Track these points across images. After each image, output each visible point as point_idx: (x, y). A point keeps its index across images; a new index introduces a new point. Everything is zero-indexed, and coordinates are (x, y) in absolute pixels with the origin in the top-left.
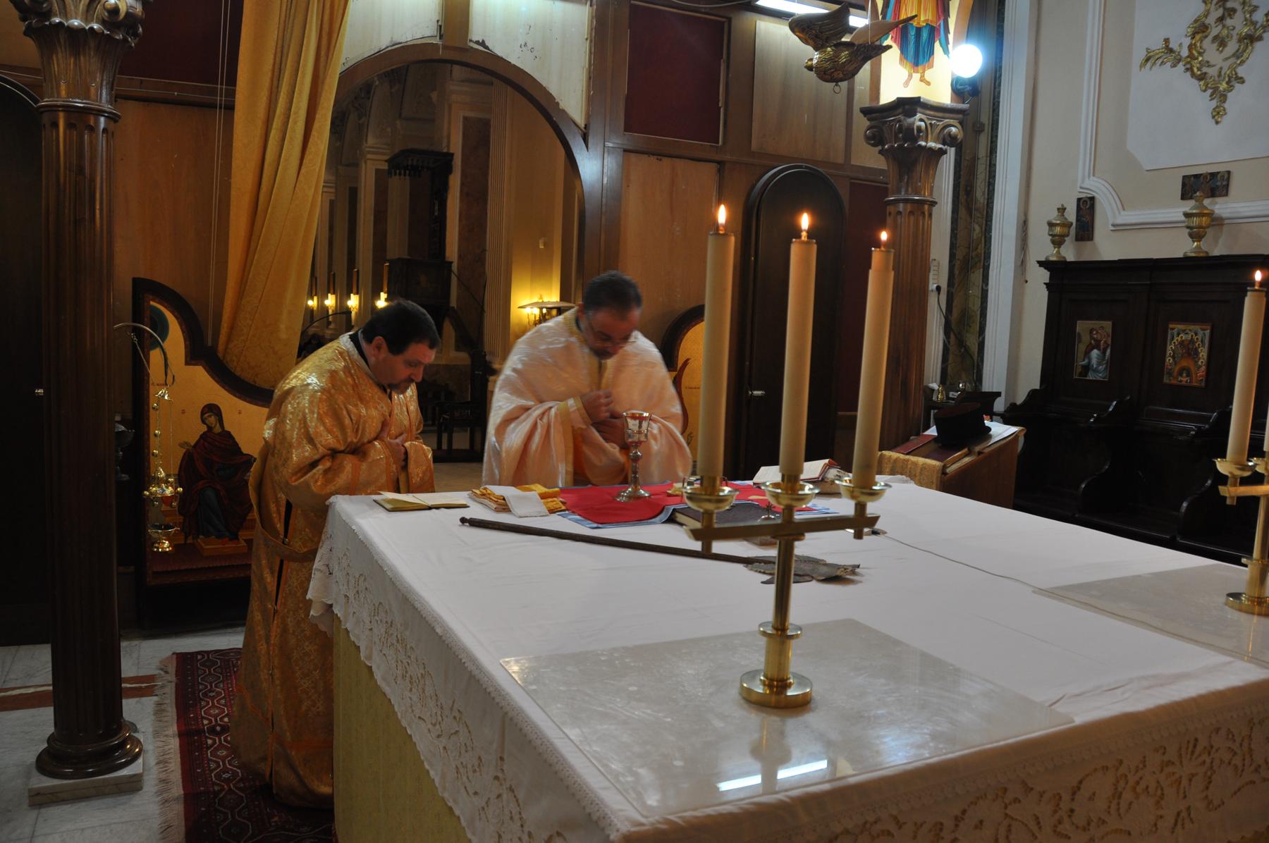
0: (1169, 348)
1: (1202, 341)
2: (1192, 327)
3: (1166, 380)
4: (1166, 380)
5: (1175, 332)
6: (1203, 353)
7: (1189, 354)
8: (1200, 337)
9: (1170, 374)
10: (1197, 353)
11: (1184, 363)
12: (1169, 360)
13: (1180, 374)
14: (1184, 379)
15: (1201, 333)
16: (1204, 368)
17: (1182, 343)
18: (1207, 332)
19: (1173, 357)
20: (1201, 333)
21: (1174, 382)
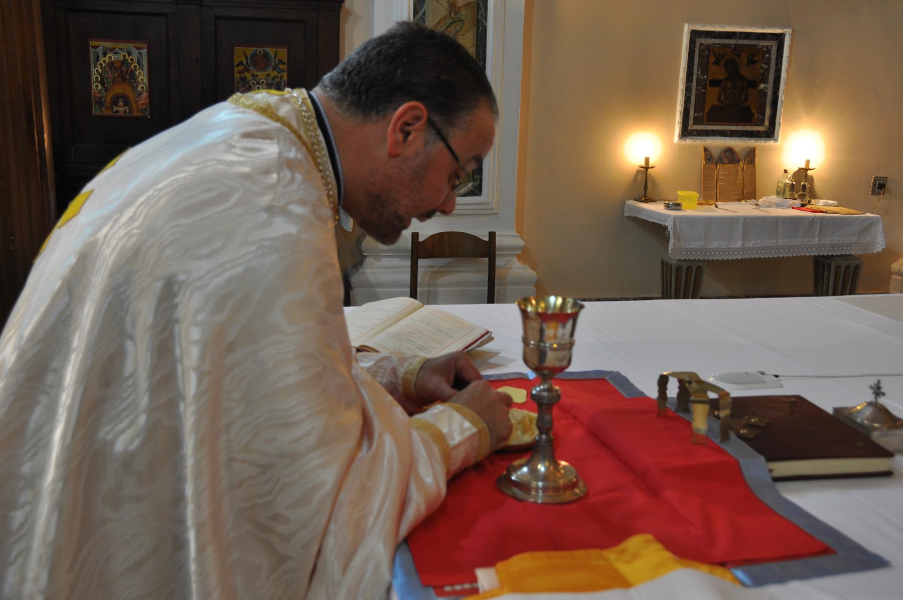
0: (94, 71)
1: (139, 62)
2: (122, 45)
3: (96, 111)
4: (96, 111)
5: (100, 50)
6: (142, 77)
7: (123, 79)
8: (135, 56)
9: (100, 103)
10: (133, 77)
11: (118, 89)
12: (96, 87)
13: (116, 104)
14: (121, 109)
15: (135, 53)
16: (145, 94)
17: (111, 65)
18: (144, 52)
19: (102, 83)
20: (135, 53)
21: (107, 113)
